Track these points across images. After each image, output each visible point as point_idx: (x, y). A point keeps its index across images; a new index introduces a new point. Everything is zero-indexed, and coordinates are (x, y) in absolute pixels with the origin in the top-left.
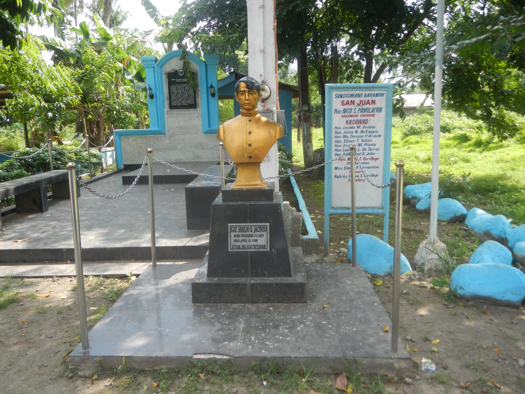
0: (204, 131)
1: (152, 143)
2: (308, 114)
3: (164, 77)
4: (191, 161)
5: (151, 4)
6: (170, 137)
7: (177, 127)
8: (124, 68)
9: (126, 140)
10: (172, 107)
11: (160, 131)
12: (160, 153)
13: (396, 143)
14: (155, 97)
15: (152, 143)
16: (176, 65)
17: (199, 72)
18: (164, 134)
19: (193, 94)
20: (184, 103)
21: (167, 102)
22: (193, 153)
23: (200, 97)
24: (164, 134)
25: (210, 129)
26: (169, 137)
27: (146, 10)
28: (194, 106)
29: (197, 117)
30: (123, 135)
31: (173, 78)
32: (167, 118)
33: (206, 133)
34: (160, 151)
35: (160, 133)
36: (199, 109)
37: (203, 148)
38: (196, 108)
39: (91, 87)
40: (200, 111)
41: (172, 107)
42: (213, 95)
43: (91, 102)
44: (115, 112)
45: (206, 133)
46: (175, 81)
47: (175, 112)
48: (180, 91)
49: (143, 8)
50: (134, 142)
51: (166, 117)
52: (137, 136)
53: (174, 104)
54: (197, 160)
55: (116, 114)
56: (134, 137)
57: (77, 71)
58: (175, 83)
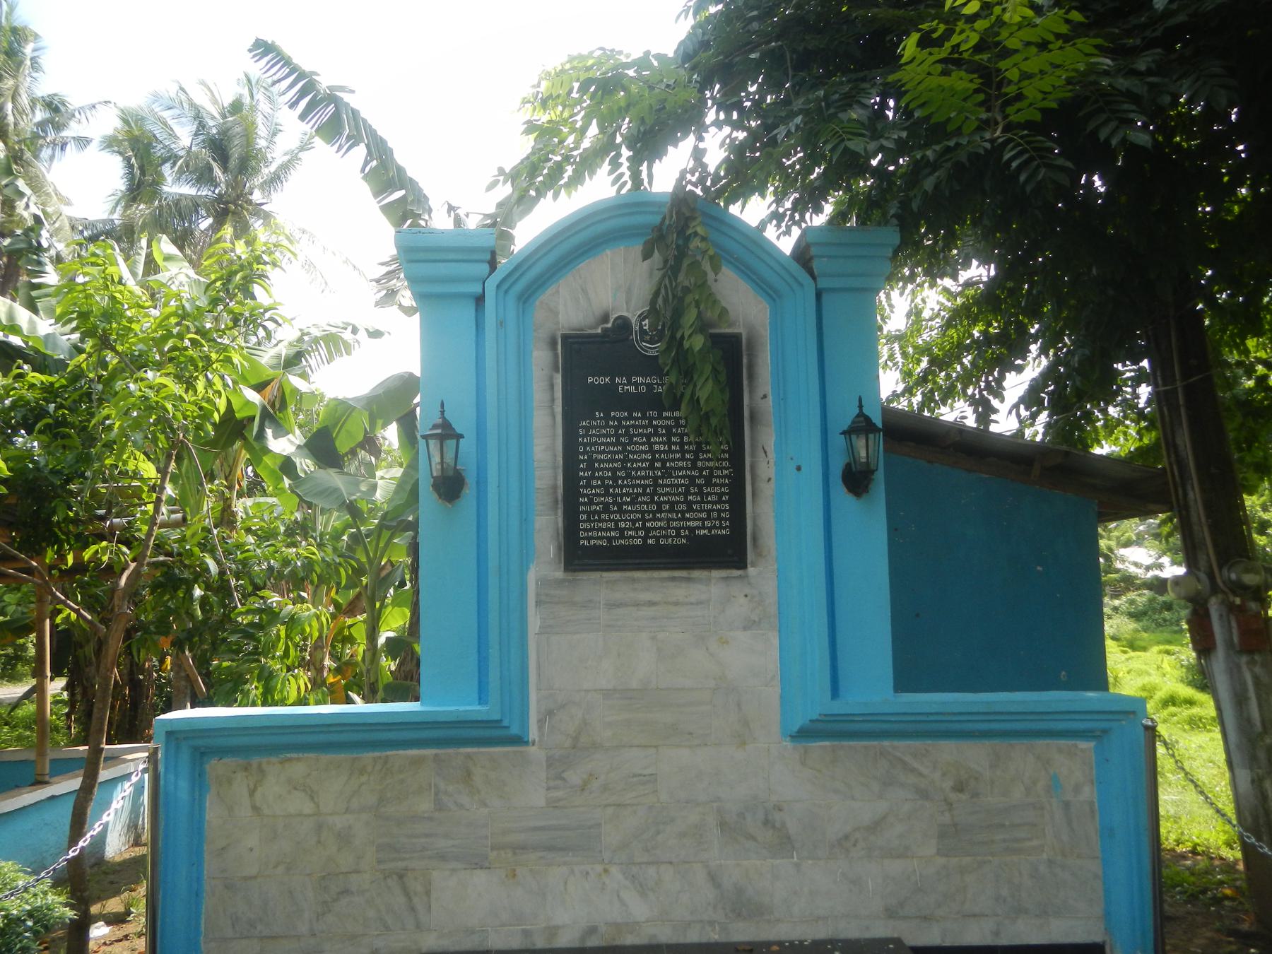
0: (797, 724)
1: (425, 805)
2: (1253, 606)
3: (540, 360)
4: (693, 937)
5: (400, 170)
6: (557, 765)
7: (607, 694)
8: (264, 408)
9: (240, 785)
10: (579, 555)
11: (496, 724)
12: (480, 877)
13: (1190, 702)
14: (469, 492)
15: (425, 805)
16: (615, 289)
17: (765, 334)
18: (519, 740)
19: (723, 473)
20: (664, 529)
21: (546, 527)
22: (713, 878)
23: (767, 490)
24: (519, 740)
25: (837, 707)
26: (550, 762)
27: (376, 194)
28: (726, 549)
29: (749, 625)
30: (222, 752)
31: (595, 366)
32: (546, 629)
33: (805, 734)
34: (478, 863)
35: (494, 734)
36: (763, 574)
37: (784, 844)
38: (741, 563)
39: (86, 459)
40: (769, 587)
41: (579, 555)
42: (857, 480)
43: (78, 537)
44: (198, 592)
45: (805, 734)
46: (614, 385)
47: (605, 587)
48: (639, 453)
49: (365, 189)
50: (298, 803)
51: (534, 622)
52: (326, 758)
53: (593, 537)
54: (742, 932)
55: (204, 601)
56: (299, 767)
57: (20, 376)
58: (609, 400)
